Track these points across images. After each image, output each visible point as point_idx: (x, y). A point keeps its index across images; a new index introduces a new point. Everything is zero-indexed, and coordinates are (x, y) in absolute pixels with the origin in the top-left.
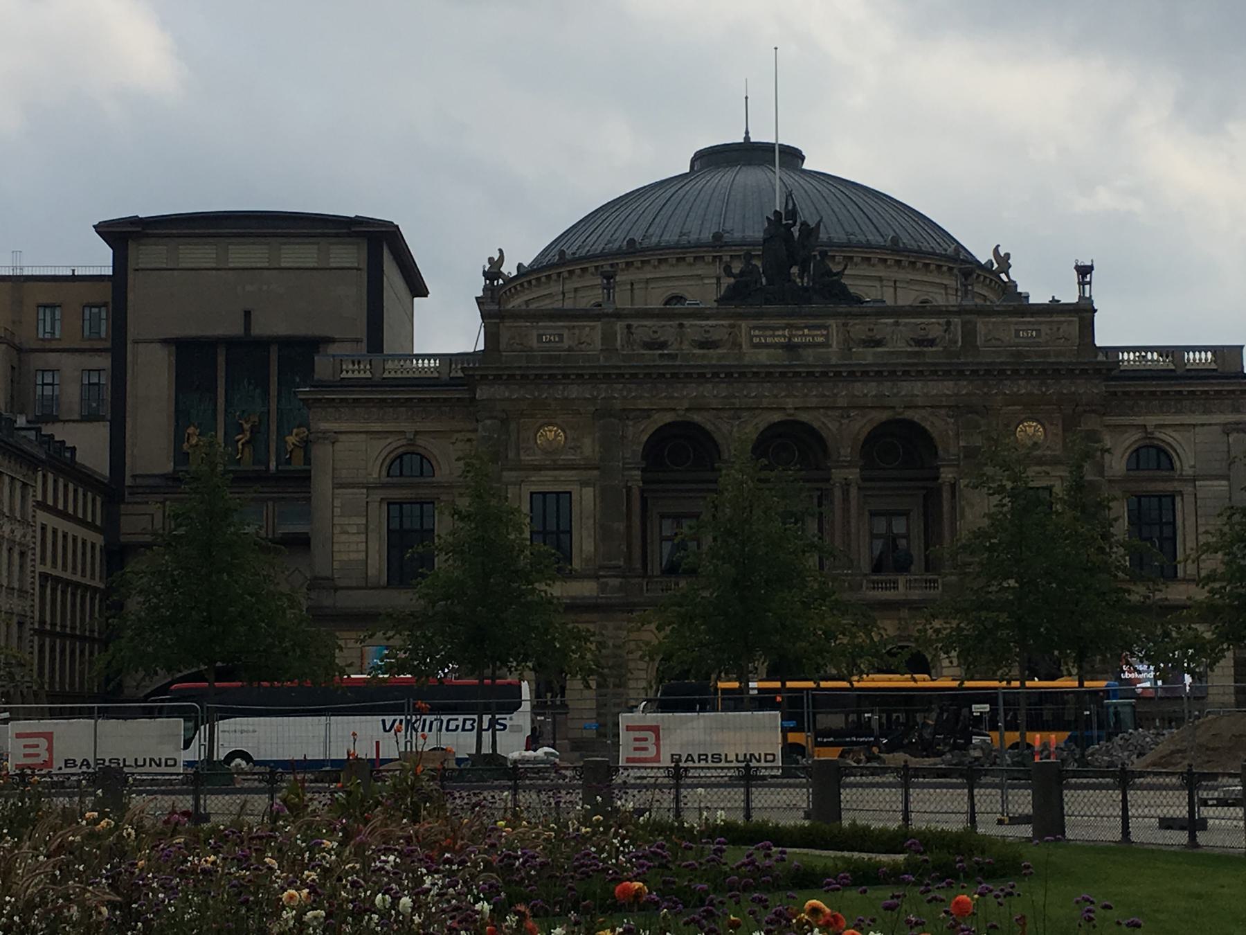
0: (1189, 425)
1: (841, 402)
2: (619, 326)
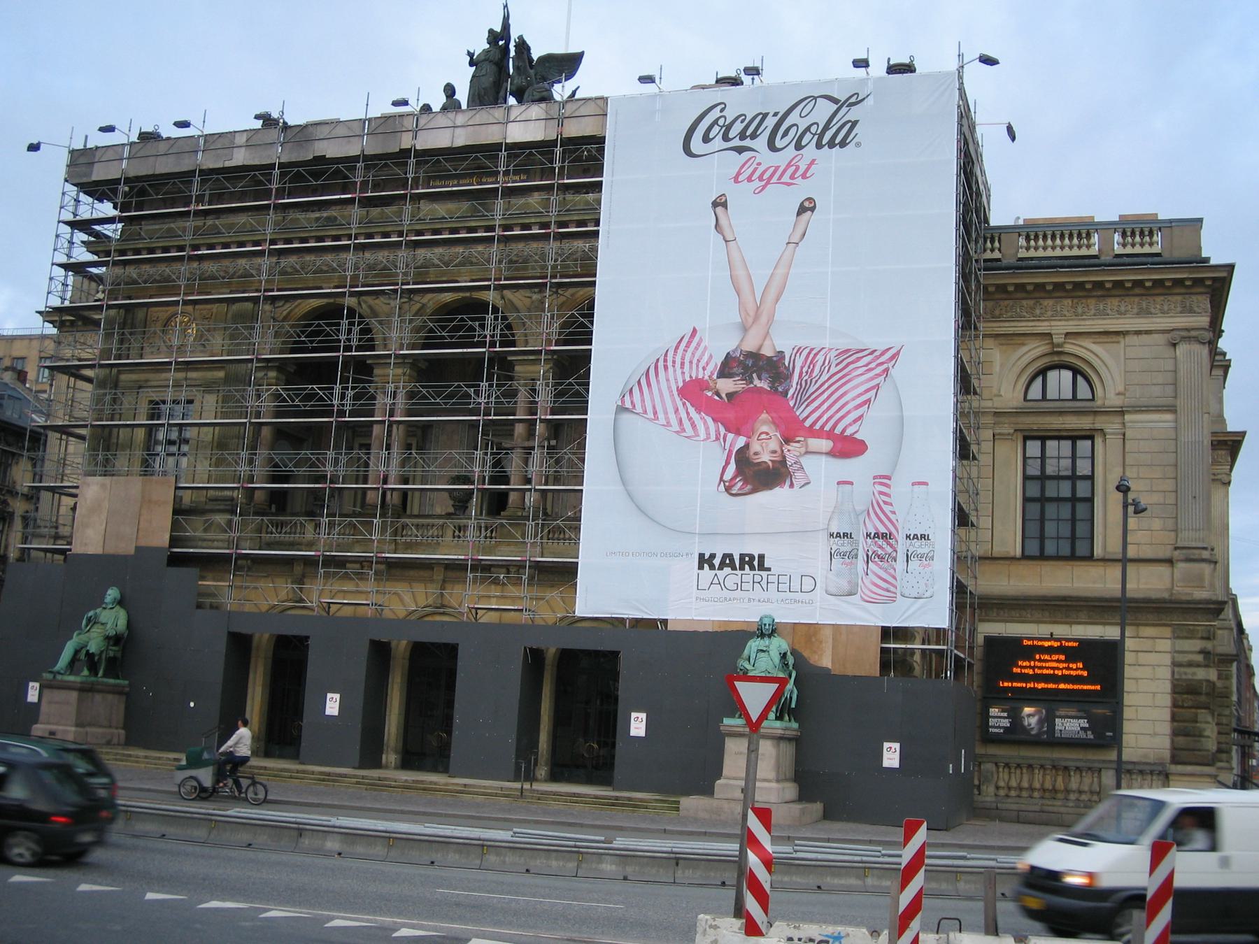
0: (1117, 333)
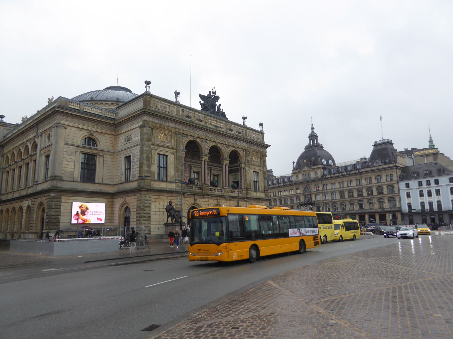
1: (227, 143)
2: (181, 109)
